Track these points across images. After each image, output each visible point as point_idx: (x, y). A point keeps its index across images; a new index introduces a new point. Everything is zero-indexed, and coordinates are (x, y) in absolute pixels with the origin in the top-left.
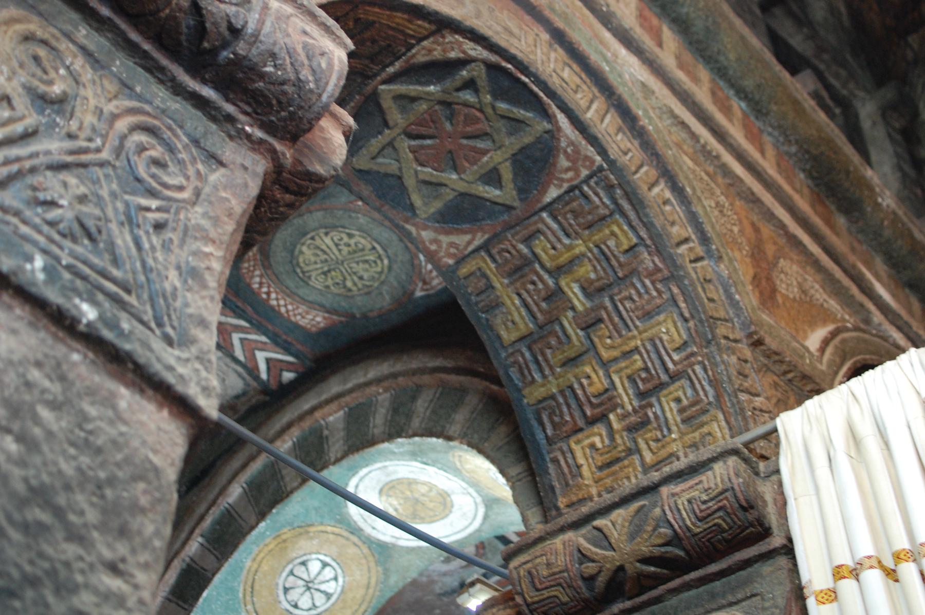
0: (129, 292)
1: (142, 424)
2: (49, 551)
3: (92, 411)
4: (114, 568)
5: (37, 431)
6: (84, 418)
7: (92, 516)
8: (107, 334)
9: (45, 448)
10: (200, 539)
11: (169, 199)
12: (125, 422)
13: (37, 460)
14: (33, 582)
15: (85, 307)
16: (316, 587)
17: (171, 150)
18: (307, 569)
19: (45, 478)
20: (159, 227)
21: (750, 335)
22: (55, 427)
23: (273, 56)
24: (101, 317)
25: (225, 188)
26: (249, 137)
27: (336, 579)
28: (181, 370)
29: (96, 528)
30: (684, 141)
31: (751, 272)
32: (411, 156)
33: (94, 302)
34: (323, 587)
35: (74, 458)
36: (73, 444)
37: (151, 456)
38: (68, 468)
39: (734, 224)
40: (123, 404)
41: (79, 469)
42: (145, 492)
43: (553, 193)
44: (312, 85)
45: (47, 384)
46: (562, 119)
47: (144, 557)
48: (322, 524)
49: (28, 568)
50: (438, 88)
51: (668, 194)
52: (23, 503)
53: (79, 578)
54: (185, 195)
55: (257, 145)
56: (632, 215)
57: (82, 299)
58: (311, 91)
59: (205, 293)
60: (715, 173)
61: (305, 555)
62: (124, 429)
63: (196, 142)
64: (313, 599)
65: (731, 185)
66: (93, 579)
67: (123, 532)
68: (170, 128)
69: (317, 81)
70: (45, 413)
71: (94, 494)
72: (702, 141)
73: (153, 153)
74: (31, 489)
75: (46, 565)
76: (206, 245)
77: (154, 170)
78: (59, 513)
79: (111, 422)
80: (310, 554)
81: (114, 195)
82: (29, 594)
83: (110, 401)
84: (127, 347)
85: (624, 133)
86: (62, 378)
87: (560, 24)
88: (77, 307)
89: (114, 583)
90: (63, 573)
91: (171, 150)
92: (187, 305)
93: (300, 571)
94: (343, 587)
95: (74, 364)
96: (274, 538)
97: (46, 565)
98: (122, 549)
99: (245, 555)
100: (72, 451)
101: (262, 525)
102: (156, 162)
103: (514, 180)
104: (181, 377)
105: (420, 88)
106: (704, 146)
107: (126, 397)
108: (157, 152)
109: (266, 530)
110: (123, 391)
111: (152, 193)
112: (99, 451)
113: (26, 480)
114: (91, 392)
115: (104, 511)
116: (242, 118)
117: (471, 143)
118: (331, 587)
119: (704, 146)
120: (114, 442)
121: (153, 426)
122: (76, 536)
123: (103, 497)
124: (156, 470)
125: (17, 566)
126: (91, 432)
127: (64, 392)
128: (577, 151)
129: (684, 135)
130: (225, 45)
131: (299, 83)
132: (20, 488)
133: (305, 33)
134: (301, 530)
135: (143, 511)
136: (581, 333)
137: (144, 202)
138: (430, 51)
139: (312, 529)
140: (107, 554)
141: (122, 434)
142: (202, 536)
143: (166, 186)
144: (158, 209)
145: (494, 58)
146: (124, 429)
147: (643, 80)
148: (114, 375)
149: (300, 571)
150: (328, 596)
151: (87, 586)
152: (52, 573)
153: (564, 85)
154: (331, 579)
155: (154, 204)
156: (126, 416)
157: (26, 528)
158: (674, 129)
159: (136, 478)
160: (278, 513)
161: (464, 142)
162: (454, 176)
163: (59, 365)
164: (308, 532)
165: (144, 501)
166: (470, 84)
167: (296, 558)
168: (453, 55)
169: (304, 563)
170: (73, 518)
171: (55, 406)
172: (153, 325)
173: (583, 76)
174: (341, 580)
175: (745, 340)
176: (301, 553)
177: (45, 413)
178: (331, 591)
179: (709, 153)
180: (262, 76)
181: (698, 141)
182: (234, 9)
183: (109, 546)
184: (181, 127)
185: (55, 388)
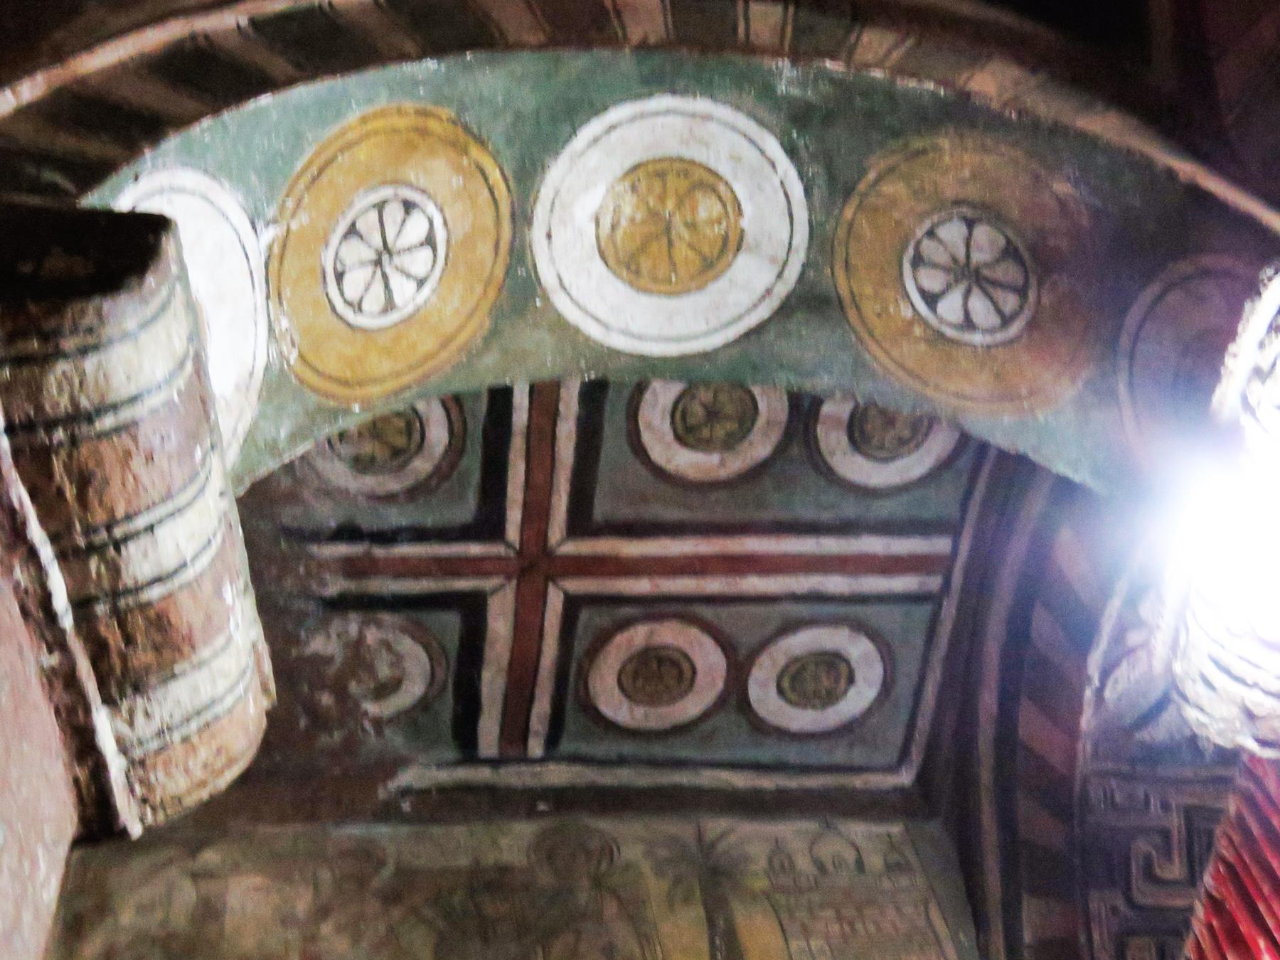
16: (388, 270)
18: (404, 221)
27: (421, 283)
34: (396, 281)
48: (495, 156)
61: (424, 191)
64: (367, 289)
80: (429, 197)
93: (394, 213)
94: (418, 310)
109: (424, 83)
118: (403, 290)
134: (462, 136)
139: (475, 152)
149: (394, 213)
150: (389, 305)
154: (415, 278)
164: (465, 151)
167: (410, 185)
169: (408, 206)
174: (427, 290)
176: (423, 183)
178: (398, 299)
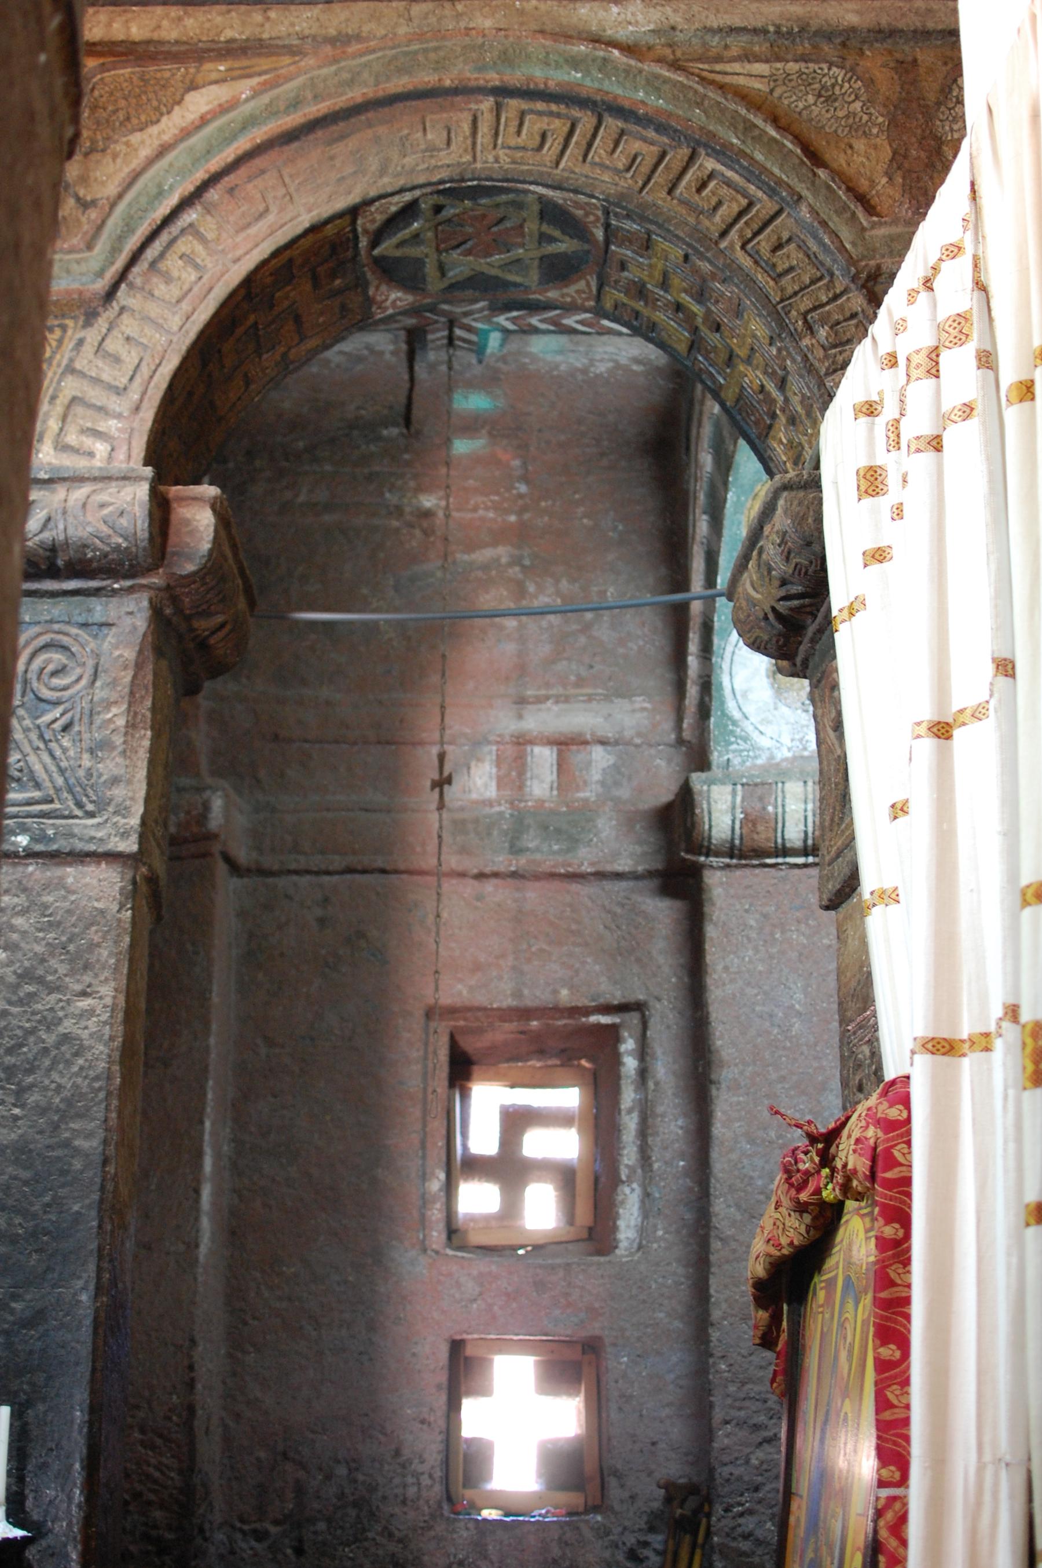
0: (52, 801)
1: (86, 885)
2: (39, 1007)
3: (51, 899)
4: (84, 994)
5: (15, 936)
6: (46, 906)
7: (62, 969)
8: (39, 847)
9: (23, 945)
10: (705, 517)
11: (71, 697)
12: (74, 892)
13: (19, 955)
14: (33, 1031)
15: (19, 838)
17: (65, 648)
19: (27, 964)
20: (66, 728)
21: (854, 279)
22: (26, 927)
23: (85, 546)
24: (33, 839)
25: (116, 647)
26: (121, 589)
28: (99, 834)
29: (66, 975)
30: (751, 43)
31: (887, 153)
32: (471, 258)
33: (24, 829)
35: (44, 939)
36: (40, 930)
37: (96, 904)
38: (39, 949)
39: (857, 98)
40: (70, 880)
41: (48, 944)
42: (97, 932)
43: (599, 234)
44: (124, 545)
45: (16, 900)
46: (532, 188)
47: (106, 974)
49: (27, 1025)
50: (421, 222)
51: (710, 164)
52: (18, 986)
53: (61, 1014)
54: (84, 682)
55: (131, 590)
56: (658, 231)
57: (16, 835)
58: (126, 548)
59: (115, 753)
60: (815, 47)
62: (73, 898)
63: (85, 625)
65: (844, 44)
66: (71, 1009)
67: (86, 967)
68: (59, 633)
69: (126, 539)
70: (19, 921)
71: (61, 954)
72: (772, 29)
73: (51, 668)
74: (19, 976)
75: (38, 1017)
76: (109, 711)
77: (56, 682)
78: (41, 980)
79: (65, 898)
81: (27, 730)
82: (32, 1039)
83: (61, 884)
84: (55, 847)
85: (630, 134)
86: (25, 890)
87: (493, 78)
88: (14, 844)
89: (84, 1003)
90: (49, 1016)
91: (65, 648)
92: (100, 775)
95: (31, 874)
96: (754, 499)
97: (38, 1017)
98: (87, 978)
99: (734, 528)
100: (41, 935)
101: (730, 495)
102: (54, 674)
103: (564, 232)
104: (101, 840)
105: (407, 231)
106: (778, 32)
107: (71, 873)
108: (57, 658)
110: (69, 870)
111: (57, 703)
112: (59, 924)
113: (15, 973)
114: (46, 887)
115: (71, 961)
116: (108, 582)
117: (501, 227)
119: (778, 32)
120: (69, 912)
121: (95, 882)
122: (52, 989)
123: (68, 952)
124: (102, 912)
125: (20, 1027)
126: (50, 915)
127: (28, 897)
128: (575, 202)
129: (745, 38)
130: (55, 557)
131: (117, 548)
132: (12, 979)
133: (102, 506)
135: (98, 945)
136: (718, 335)
137: (48, 718)
138: (373, 221)
140: (78, 987)
141: (72, 902)
142: (705, 513)
143: (65, 689)
144: (62, 715)
145: (429, 190)
146: (73, 898)
147: (652, 27)
148: (58, 864)
151: (66, 1016)
152: (43, 1021)
153: (519, 154)
155: (57, 712)
156: (73, 888)
157: (21, 1002)
158: (729, 40)
159: (87, 927)
160: (736, 479)
161: (495, 229)
162: (521, 251)
163: (20, 882)
165: (97, 939)
166: (438, 209)
168: (393, 209)
170: (50, 978)
171: (24, 912)
172: (78, 812)
173: (554, 107)
175: (853, 287)
177: (19, 921)
179: (790, 33)
180: (91, 560)
181: (765, 32)
182: (37, 538)
183: (78, 981)
184: (68, 623)
185: (21, 900)
